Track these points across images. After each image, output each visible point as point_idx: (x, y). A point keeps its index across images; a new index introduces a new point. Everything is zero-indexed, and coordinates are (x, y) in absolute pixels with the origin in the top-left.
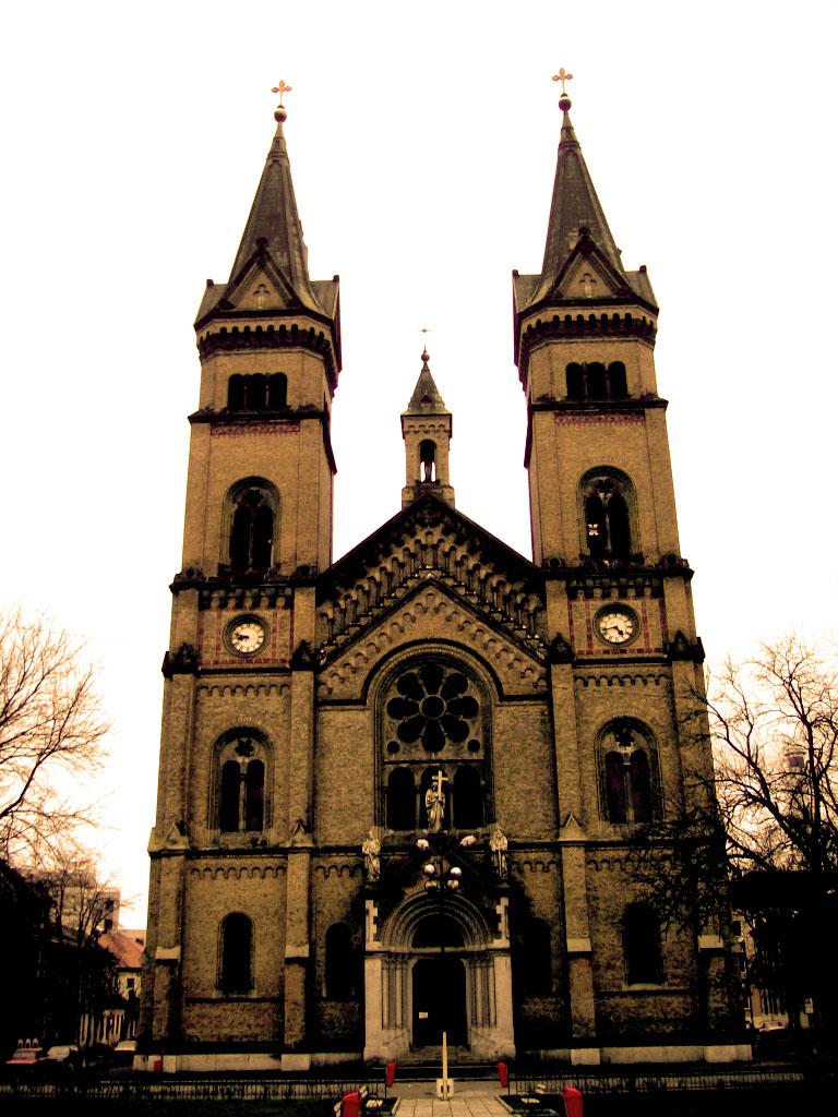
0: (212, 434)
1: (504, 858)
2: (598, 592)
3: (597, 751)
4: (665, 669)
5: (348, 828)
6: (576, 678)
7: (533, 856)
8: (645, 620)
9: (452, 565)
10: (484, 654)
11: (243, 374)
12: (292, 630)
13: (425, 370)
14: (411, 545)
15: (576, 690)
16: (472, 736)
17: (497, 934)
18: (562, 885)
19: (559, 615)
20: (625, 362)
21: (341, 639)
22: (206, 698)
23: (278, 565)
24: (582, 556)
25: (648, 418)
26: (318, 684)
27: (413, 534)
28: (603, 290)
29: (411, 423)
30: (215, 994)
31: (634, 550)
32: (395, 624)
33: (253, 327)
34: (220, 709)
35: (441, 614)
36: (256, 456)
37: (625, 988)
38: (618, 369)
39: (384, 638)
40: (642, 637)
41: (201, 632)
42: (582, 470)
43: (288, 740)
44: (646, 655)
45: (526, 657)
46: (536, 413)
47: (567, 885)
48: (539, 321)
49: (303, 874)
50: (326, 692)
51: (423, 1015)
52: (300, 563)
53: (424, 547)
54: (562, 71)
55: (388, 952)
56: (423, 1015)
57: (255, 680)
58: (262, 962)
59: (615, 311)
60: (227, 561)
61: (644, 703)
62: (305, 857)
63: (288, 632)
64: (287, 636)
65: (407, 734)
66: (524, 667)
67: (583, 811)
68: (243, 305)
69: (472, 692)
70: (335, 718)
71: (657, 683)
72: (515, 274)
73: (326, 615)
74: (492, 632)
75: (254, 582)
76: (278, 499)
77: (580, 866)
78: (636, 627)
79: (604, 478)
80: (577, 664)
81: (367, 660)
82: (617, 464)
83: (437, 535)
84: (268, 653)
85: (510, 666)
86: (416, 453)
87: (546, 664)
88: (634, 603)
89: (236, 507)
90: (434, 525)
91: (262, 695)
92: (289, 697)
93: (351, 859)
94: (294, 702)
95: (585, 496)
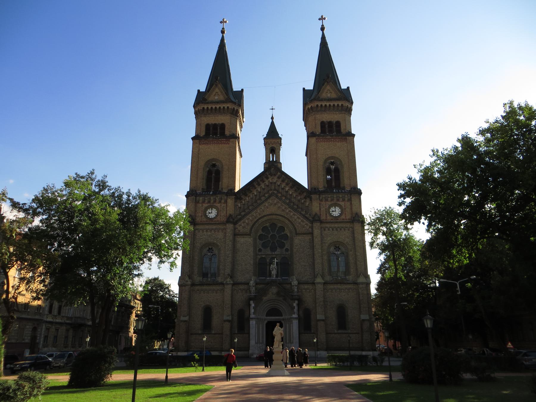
0: (200, 144)
1: (296, 287)
2: (329, 199)
4: (352, 225)
6: (321, 228)
7: (306, 287)
8: (345, 209)
9: (280, 189)
10: (291, 220)
11: (210, 123)
12: (226, 211)
15: (321, 232)
16: (286, 247)
18: (316, 297)
19: (315, 207)
20: (341, 120)
21: (243, 213)
22: (198, 233)
23: (222, 189)
24: (324, 187)
26: (235, 229)
27: (267, 178)
28: (334, 96)
29: (267, 141)
30: (200, 332)
31: (342, 186)
32: (261, 209)
33: (214, 107)
34: (202, 237)
35: (277, 206)
36: (214, 152)
37: (336, 332)
38: (338, 124)
39: (257, 214)
41: (196, 211)
44: (345, 221)
45: (305, 221)
46: (310, 138)
47: (317, 297)
48: (311, 106)
50: (238, 232)
52: (229, 188)
53: (271, 183)
54: (322, 16)
55: (258, 318)
57: (214, 227)
58: (216, 321)
60: (205, 187)
61: (344, 236)
63: (225, 211)
64: (225, 212)
66: (304, 224)
69: (287, 232)
70: (241, 240)
71: (349, 230)
72: (304, 89)
73: (238, 205)
74: (293, 212)
77: (322, 291)
79: (332, 161)
80: (321, 222)
82: (337, 156)
84: (218, 218)
86: (268, 151)
87: (312, 222)
88: (342, 203)
89: (208, 169)
90: (275, 175)
92: (225, 233)
93: (246, 287)
94: (227, 235)
95: (326, 167)
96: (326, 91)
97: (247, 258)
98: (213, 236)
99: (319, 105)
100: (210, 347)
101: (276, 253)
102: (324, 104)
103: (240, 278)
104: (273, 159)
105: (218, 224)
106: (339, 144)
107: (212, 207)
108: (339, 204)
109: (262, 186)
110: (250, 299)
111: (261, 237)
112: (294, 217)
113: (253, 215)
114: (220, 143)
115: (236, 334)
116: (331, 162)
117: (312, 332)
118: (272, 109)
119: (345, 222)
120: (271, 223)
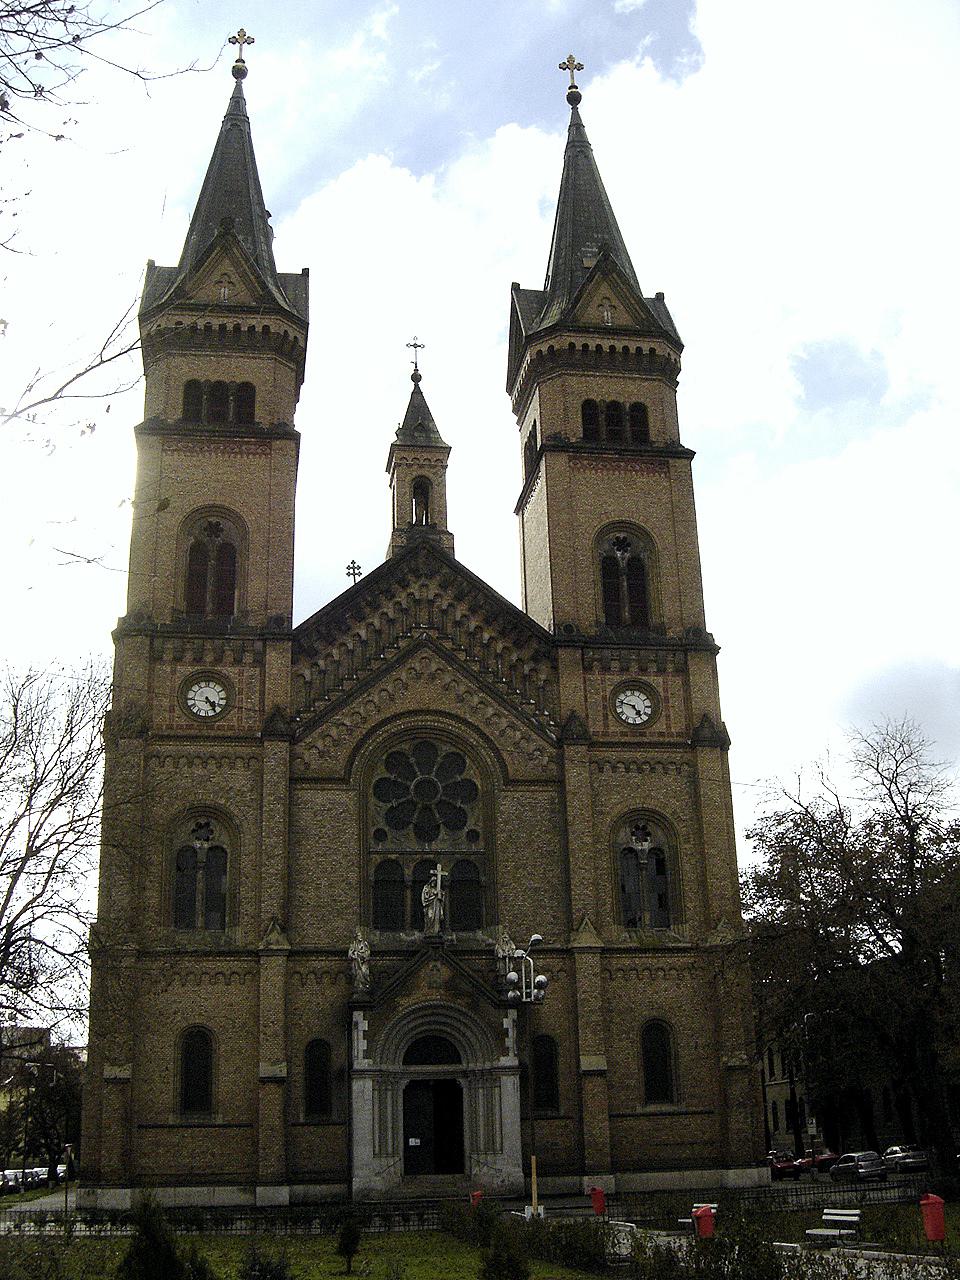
2: (615, 665)
3: (613, 845)
4: (688, 756)
5: (329, 927)
8: (667, 700)
10: (487, 731)
12: (262, 693)
13: (417, 393)
14: (402, 597)
16: (470, 825)
17: (505, 1052)
18: (574, 995)
19: (573, 690)
24: (597, 623)
25: (672, 470)
26: (293, 756)
28: (625, 319)
30: (171, 1120)
31: (654, 620)
37: (639, 1110)
38: (639, 409)
39: (371, 707)
40: (663, 719)
42: (597, 525)
43: (259, 822)
44: (667, 740)
45: (535, 736)
47: (581, 996)
48: (552, 347)
49: (279, 981)
50: (302, 768)
51: (413, 1142)
52: (273, 613)
53: (418, 602)
55: (380, 1071)
56: (413, 1142)
57: (218, 750)
58: (227, 1080)
59: (612, 342)
60: (183, 606)
61: (664, 793)
62: (281, 960)
64: (256, 698)
65: (396, 819)
66: (532, 747)
67: (597, 914)
68: (203, 296)
69: (471, 773)
70: (315, 798)
71: (679, 771)
72: (515, 287)
73: (302, 675)
74: (496, 705)
75: (217, 632)
76: (244, 537)
78: (655, 708)
79: (622, 535)
80: (592, 745)
81: (350, 731)
82: (638, 520)
83: (433, 590)
84: (233, 718)
85: (516, 744)
88: (656, 681)
90: (430, 576)
91: (226, 768)
92: (260, 773)
93: (332, 964)
96: (597, 300)
97: (334, 860)
98: (213, 780)
99: (579, 347)
100: (208, 1171)
101: (435, 846)
102: (592, 345)
103: (314, 935)
104: (419, 520)
105: (237, 739)
106: (642, 480)
107: (208, 677)
108: (646, 684)
109: (385, 610)
110: (352, 1007)
111: (382, 789)
112: (496, 724)
113: (357, 710)
114: (237, 450)
115: (303, 1125)
116: (617, 538)
117: (562, 1112)
118: (415, 346)
119: (669, 744)
120: (420, 740)
